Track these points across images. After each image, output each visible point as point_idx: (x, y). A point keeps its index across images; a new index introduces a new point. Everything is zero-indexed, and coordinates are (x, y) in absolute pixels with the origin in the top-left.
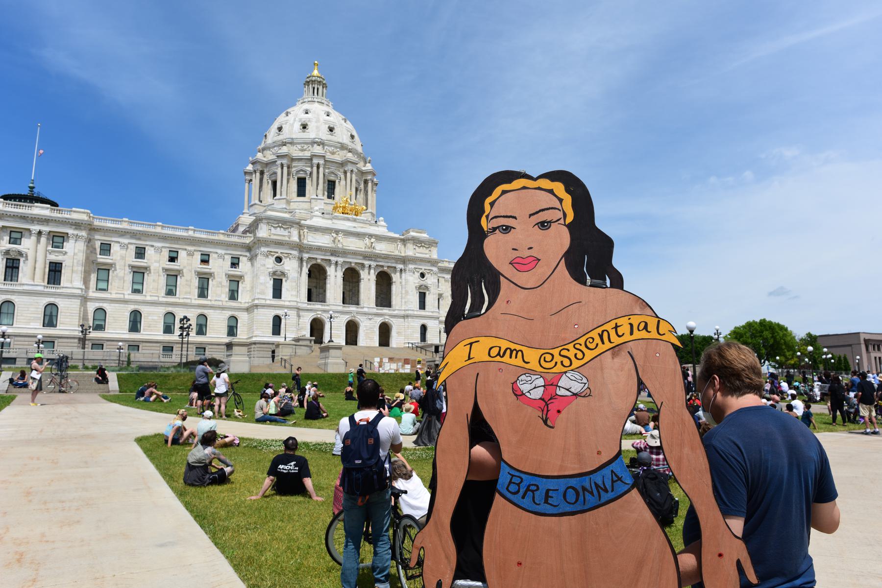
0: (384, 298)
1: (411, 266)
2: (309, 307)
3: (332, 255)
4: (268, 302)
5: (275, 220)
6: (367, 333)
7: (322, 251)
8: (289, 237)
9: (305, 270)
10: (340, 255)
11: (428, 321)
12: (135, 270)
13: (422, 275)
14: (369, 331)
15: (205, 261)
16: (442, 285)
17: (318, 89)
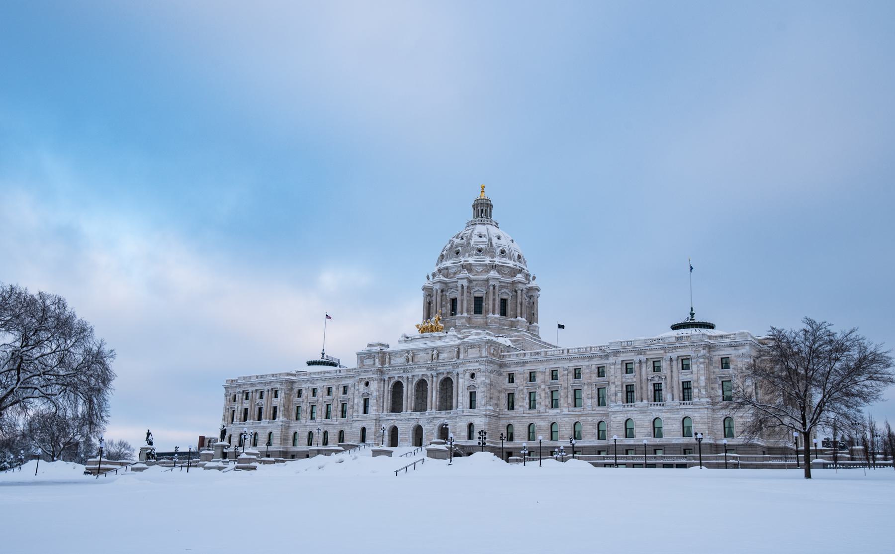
0: (446, 403)
1: (460, 370)
2: (387, 418)
3: (404, 372)
4: (360, 418)
5: (365, 354)
6: (427, 435)
7: (397, 370)
8: (374, 364)
9: (388, 388)
10: (410, 371)
11: (475, 419)
12: (312, 404)
13: (473, 376)
14: (429, 434)
15: (345, 392)
16: (516, 379)
17: (482, 210)
